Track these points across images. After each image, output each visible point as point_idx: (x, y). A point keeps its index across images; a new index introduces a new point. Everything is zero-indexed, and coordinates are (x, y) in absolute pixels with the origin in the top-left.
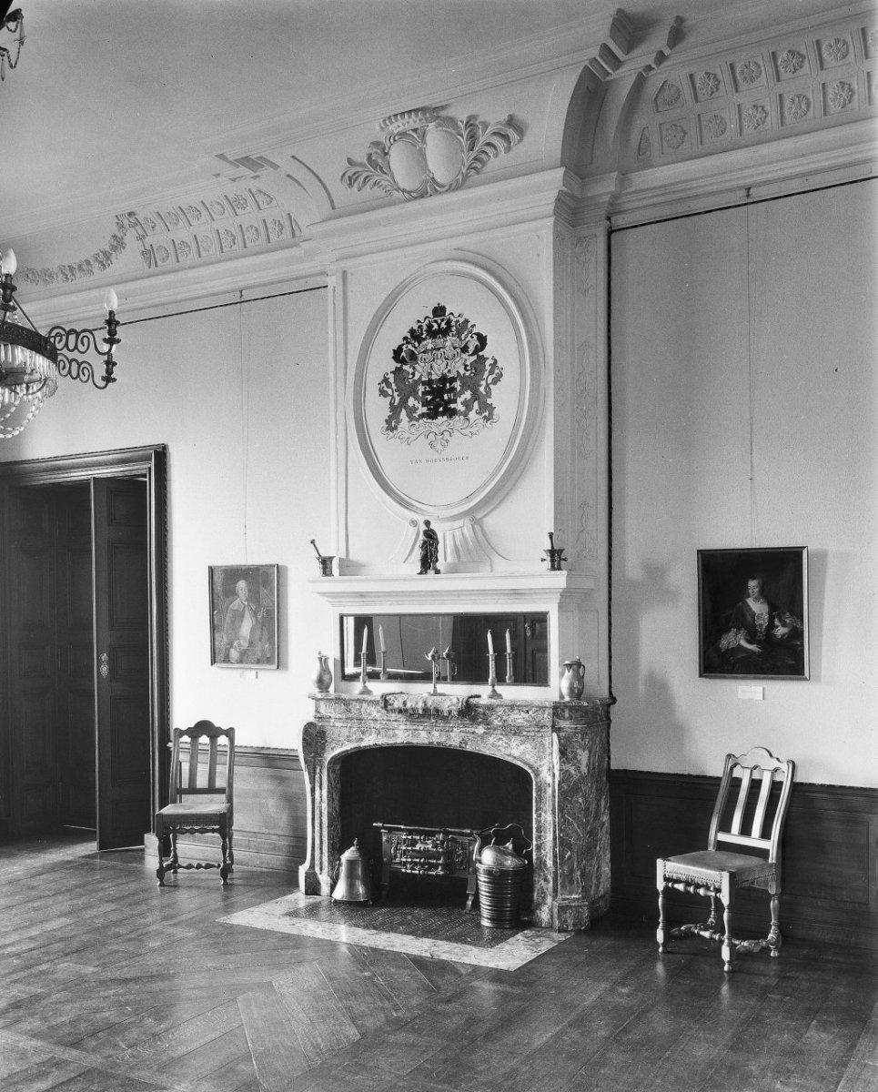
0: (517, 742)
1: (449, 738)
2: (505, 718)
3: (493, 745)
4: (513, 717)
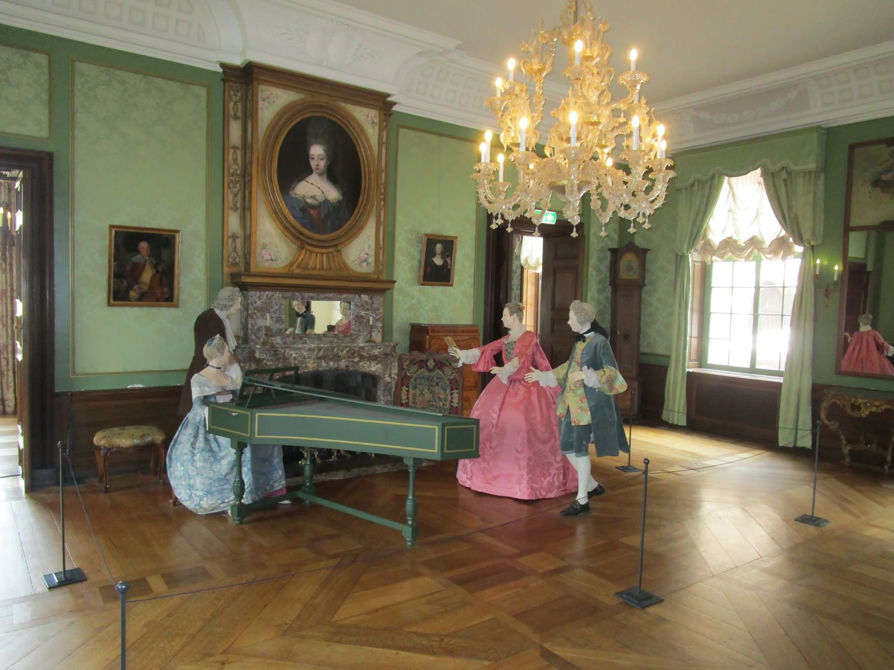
0: (375, 364)
2: (369, 352)
3: (362, 366)
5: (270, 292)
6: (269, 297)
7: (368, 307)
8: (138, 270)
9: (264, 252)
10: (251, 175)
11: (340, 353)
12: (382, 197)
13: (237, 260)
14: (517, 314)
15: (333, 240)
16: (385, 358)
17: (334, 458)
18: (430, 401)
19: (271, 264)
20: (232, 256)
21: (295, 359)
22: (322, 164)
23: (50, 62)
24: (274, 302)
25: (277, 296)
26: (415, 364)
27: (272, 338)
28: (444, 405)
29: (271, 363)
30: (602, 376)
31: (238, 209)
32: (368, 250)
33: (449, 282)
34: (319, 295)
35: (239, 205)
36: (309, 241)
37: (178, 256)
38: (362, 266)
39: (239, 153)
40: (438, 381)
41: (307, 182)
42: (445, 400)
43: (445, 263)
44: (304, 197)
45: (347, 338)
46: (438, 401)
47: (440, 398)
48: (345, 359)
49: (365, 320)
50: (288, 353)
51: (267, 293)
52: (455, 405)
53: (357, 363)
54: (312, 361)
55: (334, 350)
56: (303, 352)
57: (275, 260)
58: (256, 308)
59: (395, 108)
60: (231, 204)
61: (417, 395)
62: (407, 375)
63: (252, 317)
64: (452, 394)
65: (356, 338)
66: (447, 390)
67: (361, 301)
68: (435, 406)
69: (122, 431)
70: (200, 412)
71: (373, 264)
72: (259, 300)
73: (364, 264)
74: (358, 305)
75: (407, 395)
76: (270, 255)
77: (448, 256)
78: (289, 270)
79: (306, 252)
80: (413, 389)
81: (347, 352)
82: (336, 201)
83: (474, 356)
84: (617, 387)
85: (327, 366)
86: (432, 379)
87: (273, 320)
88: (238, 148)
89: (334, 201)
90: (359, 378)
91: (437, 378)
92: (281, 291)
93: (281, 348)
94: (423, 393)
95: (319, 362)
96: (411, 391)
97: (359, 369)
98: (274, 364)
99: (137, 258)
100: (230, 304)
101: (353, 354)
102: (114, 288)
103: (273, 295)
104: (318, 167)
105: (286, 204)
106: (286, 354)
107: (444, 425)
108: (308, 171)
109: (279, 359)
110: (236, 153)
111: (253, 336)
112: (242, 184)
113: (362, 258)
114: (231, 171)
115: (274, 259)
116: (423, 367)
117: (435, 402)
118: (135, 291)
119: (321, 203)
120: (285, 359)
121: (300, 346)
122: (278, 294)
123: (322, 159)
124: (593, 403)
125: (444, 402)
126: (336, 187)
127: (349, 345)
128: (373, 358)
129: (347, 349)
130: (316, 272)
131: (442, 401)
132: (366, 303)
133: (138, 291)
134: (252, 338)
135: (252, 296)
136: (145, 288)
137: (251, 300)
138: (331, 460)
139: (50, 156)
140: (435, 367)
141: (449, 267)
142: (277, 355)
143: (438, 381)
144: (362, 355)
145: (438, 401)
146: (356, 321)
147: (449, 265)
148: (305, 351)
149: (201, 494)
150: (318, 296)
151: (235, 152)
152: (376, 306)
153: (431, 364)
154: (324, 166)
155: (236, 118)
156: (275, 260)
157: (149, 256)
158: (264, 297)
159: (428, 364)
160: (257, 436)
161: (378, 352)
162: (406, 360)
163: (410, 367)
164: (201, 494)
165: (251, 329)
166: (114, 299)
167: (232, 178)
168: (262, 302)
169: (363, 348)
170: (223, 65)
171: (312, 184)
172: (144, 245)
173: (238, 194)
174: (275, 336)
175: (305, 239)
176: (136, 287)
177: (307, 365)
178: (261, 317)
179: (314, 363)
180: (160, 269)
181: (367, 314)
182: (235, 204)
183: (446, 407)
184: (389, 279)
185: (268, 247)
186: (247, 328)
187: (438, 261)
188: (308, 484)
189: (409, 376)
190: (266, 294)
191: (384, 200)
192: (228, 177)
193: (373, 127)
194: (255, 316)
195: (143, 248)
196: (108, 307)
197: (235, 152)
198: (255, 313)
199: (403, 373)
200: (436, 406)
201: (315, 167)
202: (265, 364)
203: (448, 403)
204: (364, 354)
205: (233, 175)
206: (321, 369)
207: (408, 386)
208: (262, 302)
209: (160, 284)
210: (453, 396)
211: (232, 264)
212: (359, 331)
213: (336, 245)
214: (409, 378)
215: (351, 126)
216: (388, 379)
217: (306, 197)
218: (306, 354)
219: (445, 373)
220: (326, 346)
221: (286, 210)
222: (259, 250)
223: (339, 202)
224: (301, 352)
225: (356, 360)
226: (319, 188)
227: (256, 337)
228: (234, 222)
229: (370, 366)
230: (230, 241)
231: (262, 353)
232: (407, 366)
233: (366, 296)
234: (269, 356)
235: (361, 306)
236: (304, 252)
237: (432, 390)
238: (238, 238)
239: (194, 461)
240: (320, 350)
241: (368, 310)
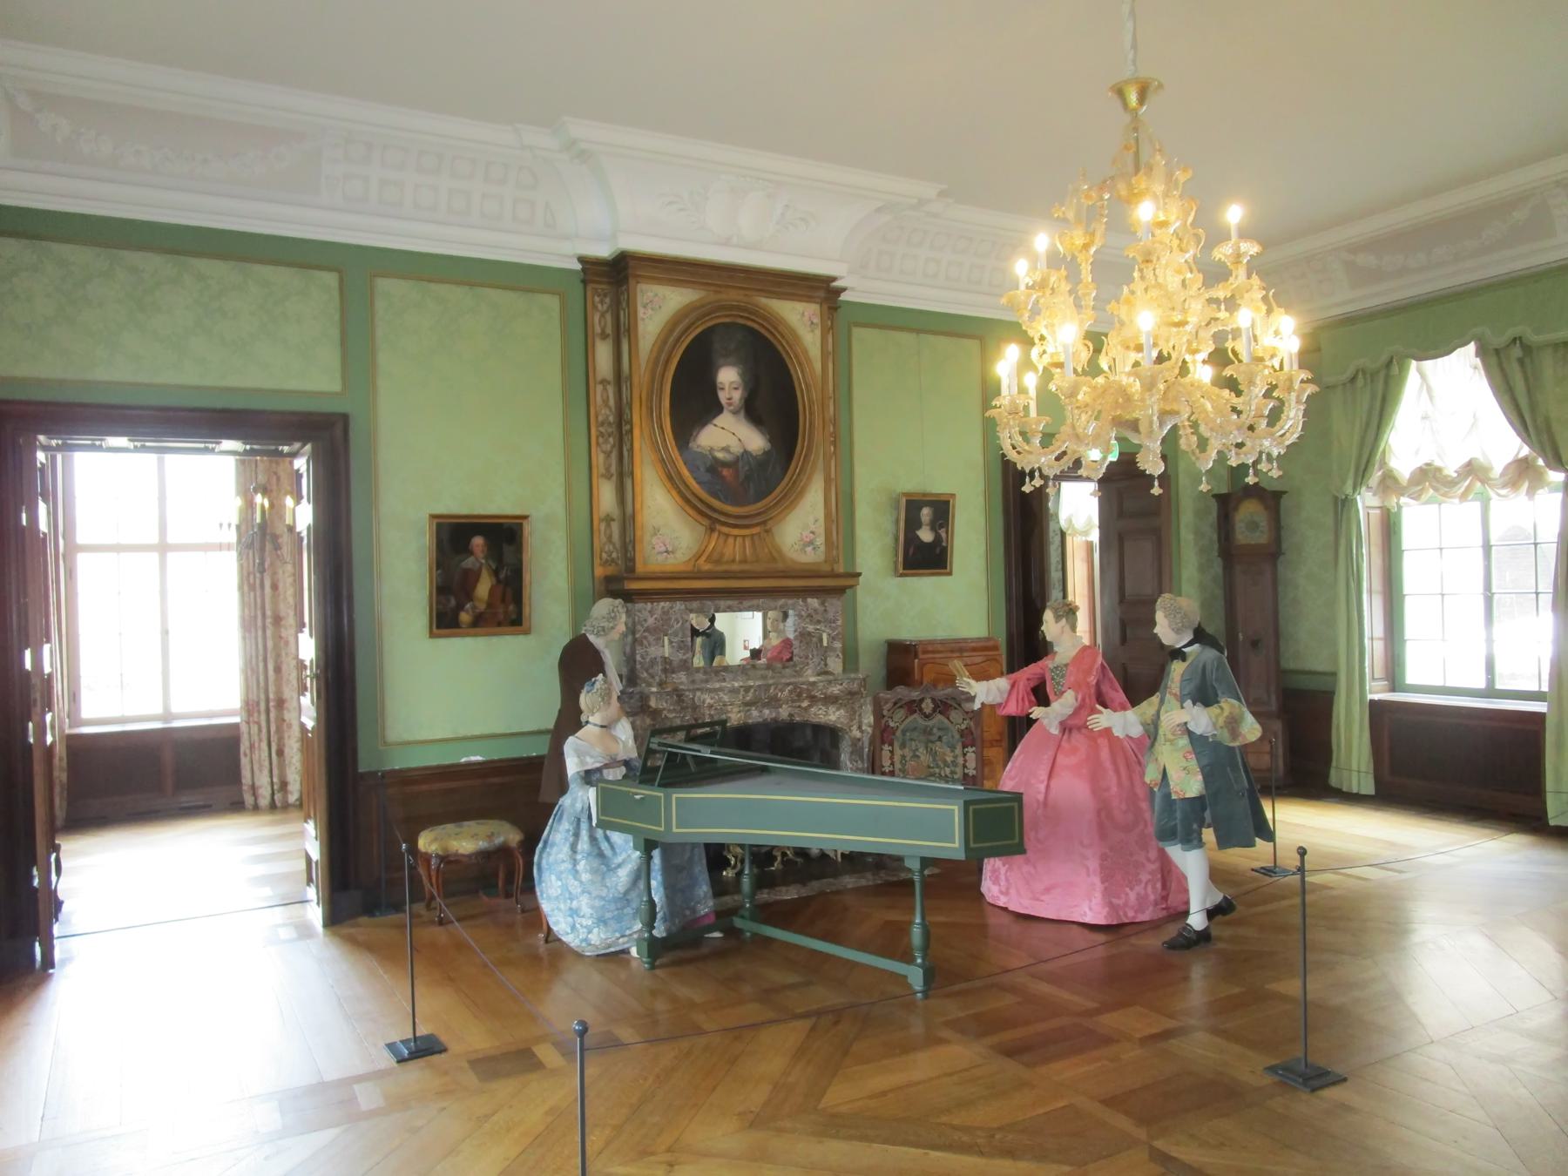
0: (834, 709)
2: (824, 691)
6: (666, 609)
7: (819, 617)
8: (470, 578)
9: (654, 541)
10: (630, 422)
11: (780, 694)
12: (832, 439)
13: (614, 555)
15: (759, 514)
16: (851, 699)
17: (777, 866)
18: (929, 767)
19: (666, 558)
20: (607, 549)
21: (710, 706)
22: (737, 396)
23: (341, 281)
25: (677, 608)
26: (901, 707)
27: (674, 676)
28: (953, 772)
31: (612, 475)
32: (814, 526)
33: (946, 568)
34: (741, 603)
35: (613, 469)
36: (722, 519)
39: (611, 390)
40: (940, 733)
41: (715, 425)
42: (954, 763)
43: (938, 539)
44: (712, 449)
45: (787, 670)
46: (942, 766)
47: (945, 762)
49: (814, 639)
51: (662, 604)
52: (972, 772)
53: (806, 709)
54: (736, 710)
57: (673, 552)
58: (647, 630)
59: (844, 297)
60: (602, 470)
61: (908, 759)
63: (641, 644)
64: (965, 755)
65: (801, 669)
66: (955, 748)
69: (458, 830)
70: (582, 796)
71: (823, 548)
72: (652, 616)
73: (809, 549)
74: (802, 616)
75: (892, 758)
76: (665, 546)
77: (941, 526)
78: (694, 565)
79: (719, 535)
80: (901, 749)
81: (790, 692)
82: (760, 453)
83: (999, 689)
87: (673, 647)
88: (609, 383)
90: (809, 732)
91: (939, 729)
92: (684, 600)
93: (689, 690)
94: (917, 753)
96: (898, 752)
97: (811, 719)
99: (469, 562)
100: (611, 625)
101: (799, 695)
102: (437, 609)
103: (672, 608)
105: (685, 464)
106: (696, 699)
107: (967, 804)
108: (717, 408)
112: (618, 436)
113: (805, 539)
114: (600, 418)
115: (670, 549)
116: (915, 712)
118: (467, 612)
119: (737, 460)
120: (695, 708)
121: (717, 685)
122: (679, 606)
123: (736, 389)
124: (1205, 761)
125: (953, 768)
126: (761, 431)
127: (792, 680)
128: (830, 700)
129: (789, 688)
130: (735, 567)
131: (948, 767)
132: (815, 610)
133: (471, 612)
135: (640, 611)
136: (482, 607)
137: (639, 617)
138: (773, 868)
139: (345, 418)
140: (934, 710)
141: (944, 544)
142: (683, 701)
143: (940, 733)
144: (814, 697)
145: (942, 766)
146: (801, 642)
148: (725, 694)
149: (590, 923)
150: (740, 605)
151: (605, 389)
152: (830, 615)
154: (741, 399)
155: (604, 336)
157: (486, 558)
158: (659, 612)
159: (923, 706)
160: (675, 830)
164: (590, 923)
165: (641, 663)
167: (602, 429)
169: (814, 684)
170: (582, 260)
171: (723, 428)
172: (478, 542)
173: (611, 452)
175: (715, 515)
176: (468, 606)
177: (729, 715)
178: (654, 643)
179: (740, 712)
180: (502, 576)
181: (818, 629)
182: (608, 469)
183: (956, 777)
184: (850, 571)
186: (635, 661)
187: (926, 535)
188: (748, 905)
190: (660, 607)
191: (834, 443)
192: (597, 427)
193: (812, 331)
194: (645, 642)
195: (478, 546)
197: (605, 389)
198: (645, 638)
199: (883, 722)
203: (959, 770)
205: (602, 424)
206: (750, 721)
207: (891, 744)
208: (656, 619)
209: (503, 601)
210: (967, 757)
211: (607, 561)
212: (807, 658)
213: (764, 523)
214: (893, 731)
215: (779, 332)
216: (856, 733)
218: (726, 698)
219: (953, 720)
220: (758, 683)
221: (686, 473)
222: (647, 537)
223: (766, 453)
224: (718, 695)
225: (805, 704)
226: (734, 434)
228: (607, 496)
229: (827, 714)
230: (603, 526)
232: (889, 711)
233: (815, 600)
234: (671, 704)
235: (807, 616)
236: (715, 535)
237: (931, 749)
238: (613, 520)
239: (577, 872)
241: (819, 622)
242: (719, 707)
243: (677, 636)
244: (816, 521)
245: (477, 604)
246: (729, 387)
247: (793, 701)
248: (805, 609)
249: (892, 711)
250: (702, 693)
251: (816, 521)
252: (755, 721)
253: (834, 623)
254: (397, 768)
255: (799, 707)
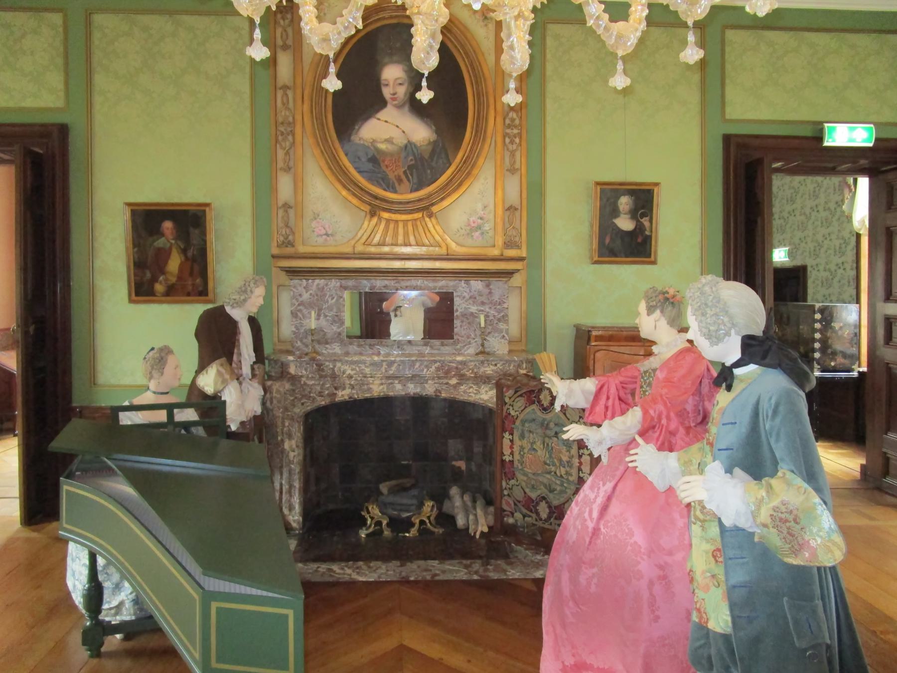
0: (487, 389)
1: (424, 388)
2: (475, 370)
3: (465, 392)
4: (482, 369)
5: (323, 280)
7: (484, 299)
8: (162, 256)
14: (662, 312)
18: (545, 463)
19: (326, 240)
21: (350, 377)
24: (328, 293)
25: (332, 285)
26: (521, 396)
27: (327, 346)
28: (567, 473)
29: (313, 382)
30: (759, 503)
32: (482, 213)
33: (649, 256)
37: (212, 238)
38: (472, 236)
41: (379, 119)
43: (639, 229)
44: (374, 141)
46: (558, 465)
47: (560, 460)
48: (433, 379)
50: (340, 368)
51: (317, 281)
53: (455, 387)
54: (378, 382)
55: (414, 365)
56: (363, 368)
57: (332, 235)
62: (510, 414)
64: (580, 456)
67: (470, 291)
68: (553, 473)
72: (307, 292)
73: (477, 234)
75: (511, 447)
76: (324, 229)
77: (643, 215)
80: (520, 439)
81: (438, 369)
82: (426, 142)
83: (583, 392)
84: (813, 543)
85: (402, 390)
86: (548, 424)
87: (328, 320)
89: (422, 143)
91: (556, 425)
93: (329, 361)
95: (392, 383)
96: (518, 442)
98: (319, 384)
99: (161, 242)
100: (242, 298)
101: (447, 372)
102: (135, 280)
103: (327, 285)
104: (396, 96)
106: (336, 369)
109: (326, 376)
110: (286, 94)
111: (299, 342)
113: (473, 225)
115: (330, 233)
116: (534, 403)
117: (553, 466)
118: (161, 283)
122: (334, 283)
124: (740, 576)
125: (568, 469)
126: (426, 123)
131: (564, 467)
134: (297, 345)
135: (295, 287)
136: (173, 280)
139: (63, 130)
141: (647, 233)
142: (323, 370)
145: (558, 465)
147: (648, 229)
148: (366, 367)
152: (496, 297)
153: (545, 397)
154: (405, 94)
156: (332, 235)
157: (175, 239)
158: (314, 287)
161: (492, 370)
162: (509, 387)
163: (513, 401)
166: (137, 294)
168: (311, 294)
171: (386, 122)
172: (168, 226)
174: (331, 343)
176: (161, 278)
177: (371, 386)
179: (382, 384)
180: (190, 254)
185: (320, 217)
189: (513, 416)
194: (300, 315)
195: (168, 229)
196: (133, 306)
198: (300, 311)
200: (555, 473)
201: (392, 96)
202: (305, 384)
203: (574, 472)
204: (467, 373)
207: (512, 434)
208: (311, 294)
209: (191, 274)
210: (582, 460)
217: (377, 142)
218: (368, 371)
219: (568, 415)
224: (359, 367)
225: (454, 381)
226: (397, 126)
227: (304, 344)
229: (478, 392)
231: (299, 367)
234: (311, 373)
235: (471, 297)
236: (375, 220)
237: (548, 444)
240: (390, 364)
241: (483, 303)
242: (359, 379)
243: (331, 310)
244: (485, 207)
245: (170, 278)
246: (394, 84)
247: (439, 378)
248: (468, 291)
249: (512, 399)
250: (342, 364)
251: (485, 207)
252: (396, 394)
253: (500, 304)
254: (103, 405)
255: (447, 384)
